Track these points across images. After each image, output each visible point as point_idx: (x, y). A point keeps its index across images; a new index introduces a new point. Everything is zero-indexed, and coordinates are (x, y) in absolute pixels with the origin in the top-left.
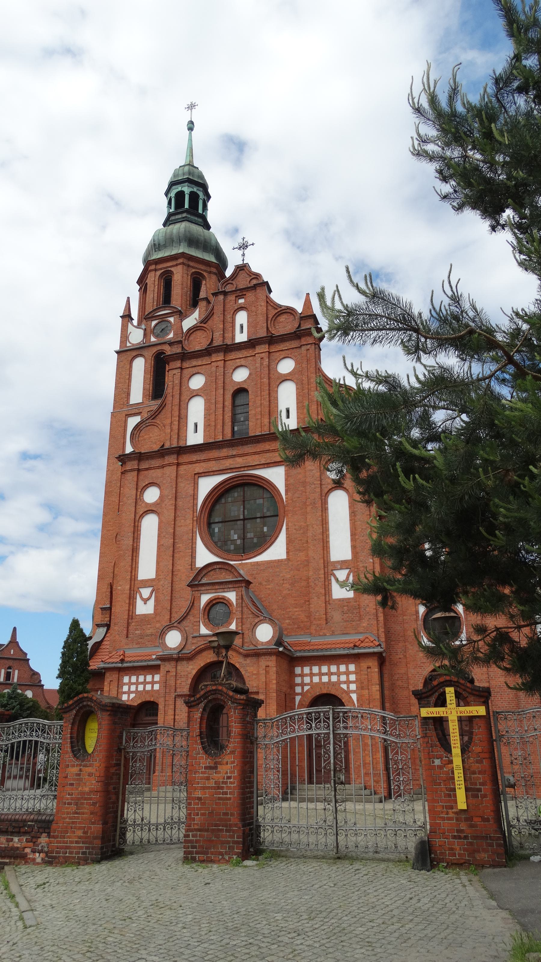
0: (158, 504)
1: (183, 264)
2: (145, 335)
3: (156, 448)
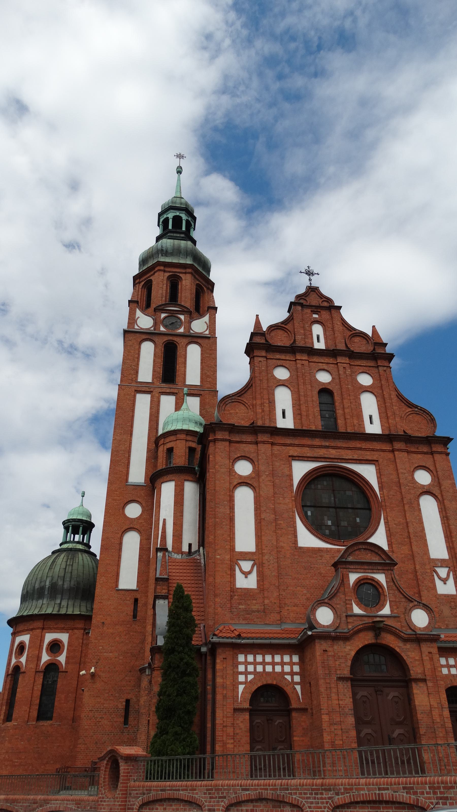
0: (253, 478)
1: (191, 273)
2: (156, 324)
3: (245, 423)
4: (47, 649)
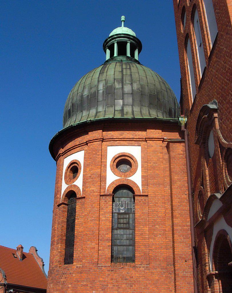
4: (112, 166)
